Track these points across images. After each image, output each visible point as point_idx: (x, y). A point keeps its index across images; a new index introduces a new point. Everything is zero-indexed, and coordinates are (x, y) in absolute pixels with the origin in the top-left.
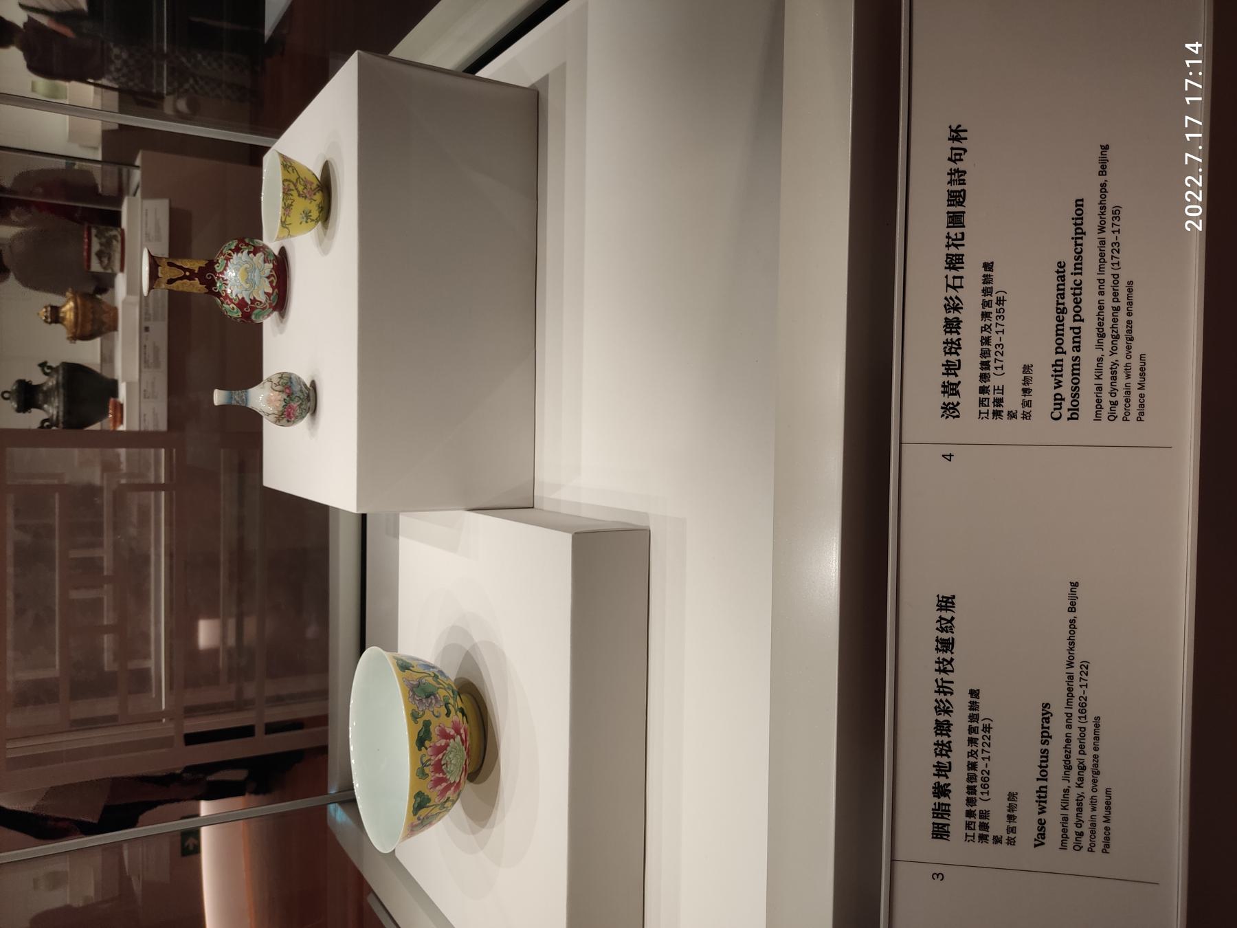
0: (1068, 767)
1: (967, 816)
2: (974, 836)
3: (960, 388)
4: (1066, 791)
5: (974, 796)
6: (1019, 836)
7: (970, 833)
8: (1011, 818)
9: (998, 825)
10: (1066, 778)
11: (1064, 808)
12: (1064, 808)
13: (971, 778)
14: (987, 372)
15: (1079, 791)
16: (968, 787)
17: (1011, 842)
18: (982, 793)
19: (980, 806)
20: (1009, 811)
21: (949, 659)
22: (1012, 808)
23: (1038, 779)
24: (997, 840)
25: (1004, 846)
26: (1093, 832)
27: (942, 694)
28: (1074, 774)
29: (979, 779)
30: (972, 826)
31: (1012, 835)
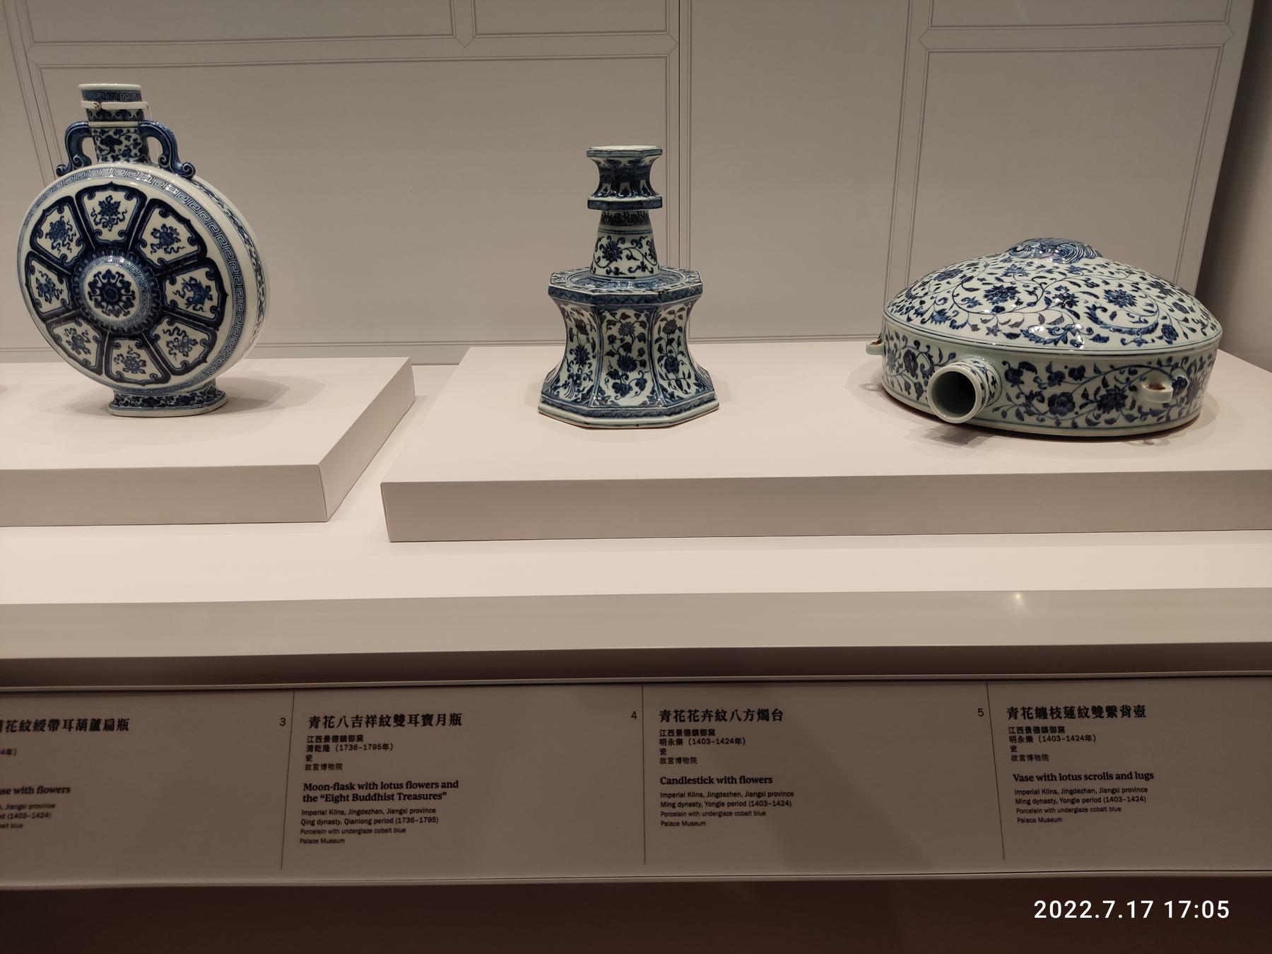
1: (326, 736)
2: (311, 742)
3: (428, 726)
6: (312, 772)
7: (314, 740)
8: (324, 766)
9: (319, 758)
13: (352, 738)
14: (691, 734)
16: (345, 736)
17: (308, 767)
18: (341, 746)
19: (332, 745)
21: (389, 723)
23: (382, 783)
24: (309, 758)
25: (305, 762)
29: (351, 743)
31: (312, 768)
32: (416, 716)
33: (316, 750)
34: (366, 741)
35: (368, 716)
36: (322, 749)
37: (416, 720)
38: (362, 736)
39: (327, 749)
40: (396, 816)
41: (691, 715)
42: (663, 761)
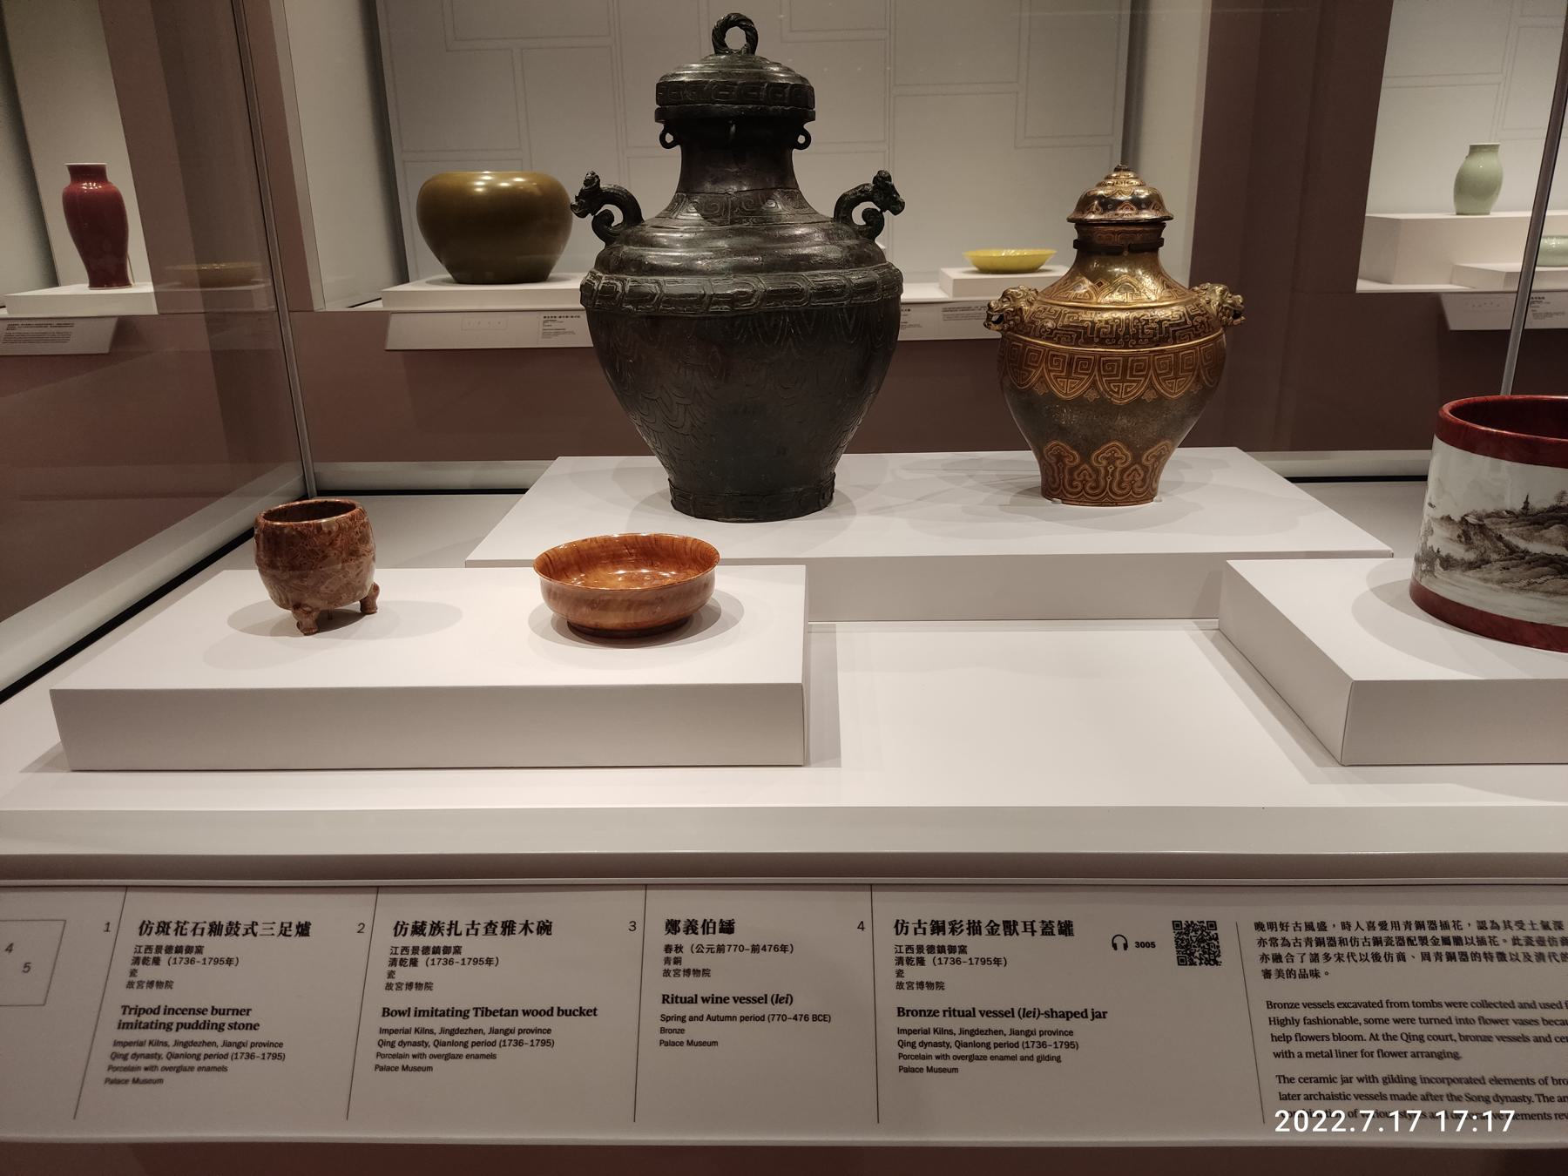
0: (452, 1032)
2: (396, 954)
4: (431, 1032)
5: (431, 952)
6: (394, 993)
7: (399, 951)
9: (404, 974)
10: (443, 1031)
11: (416, 1030)
12: (416, 1030)
15: (431, 1044)
17: (389, 987)
18: (433, 960)
20: (416, 984)
22: (419, 986)
24: (391, 974)
26: (394, 1056)
27: (448, 927)
28: (446, 1038)
30: (404, 952)
32: (1032, 923)
33: (401, 965)
34: (465, 954)
35: (969, 921)
36: (408, 963)
37: (1032, 928)
38: (459, 947)
39: (414, 962)
40: (1022, 1038)
41: (969, 927)
42: (900, 986)
